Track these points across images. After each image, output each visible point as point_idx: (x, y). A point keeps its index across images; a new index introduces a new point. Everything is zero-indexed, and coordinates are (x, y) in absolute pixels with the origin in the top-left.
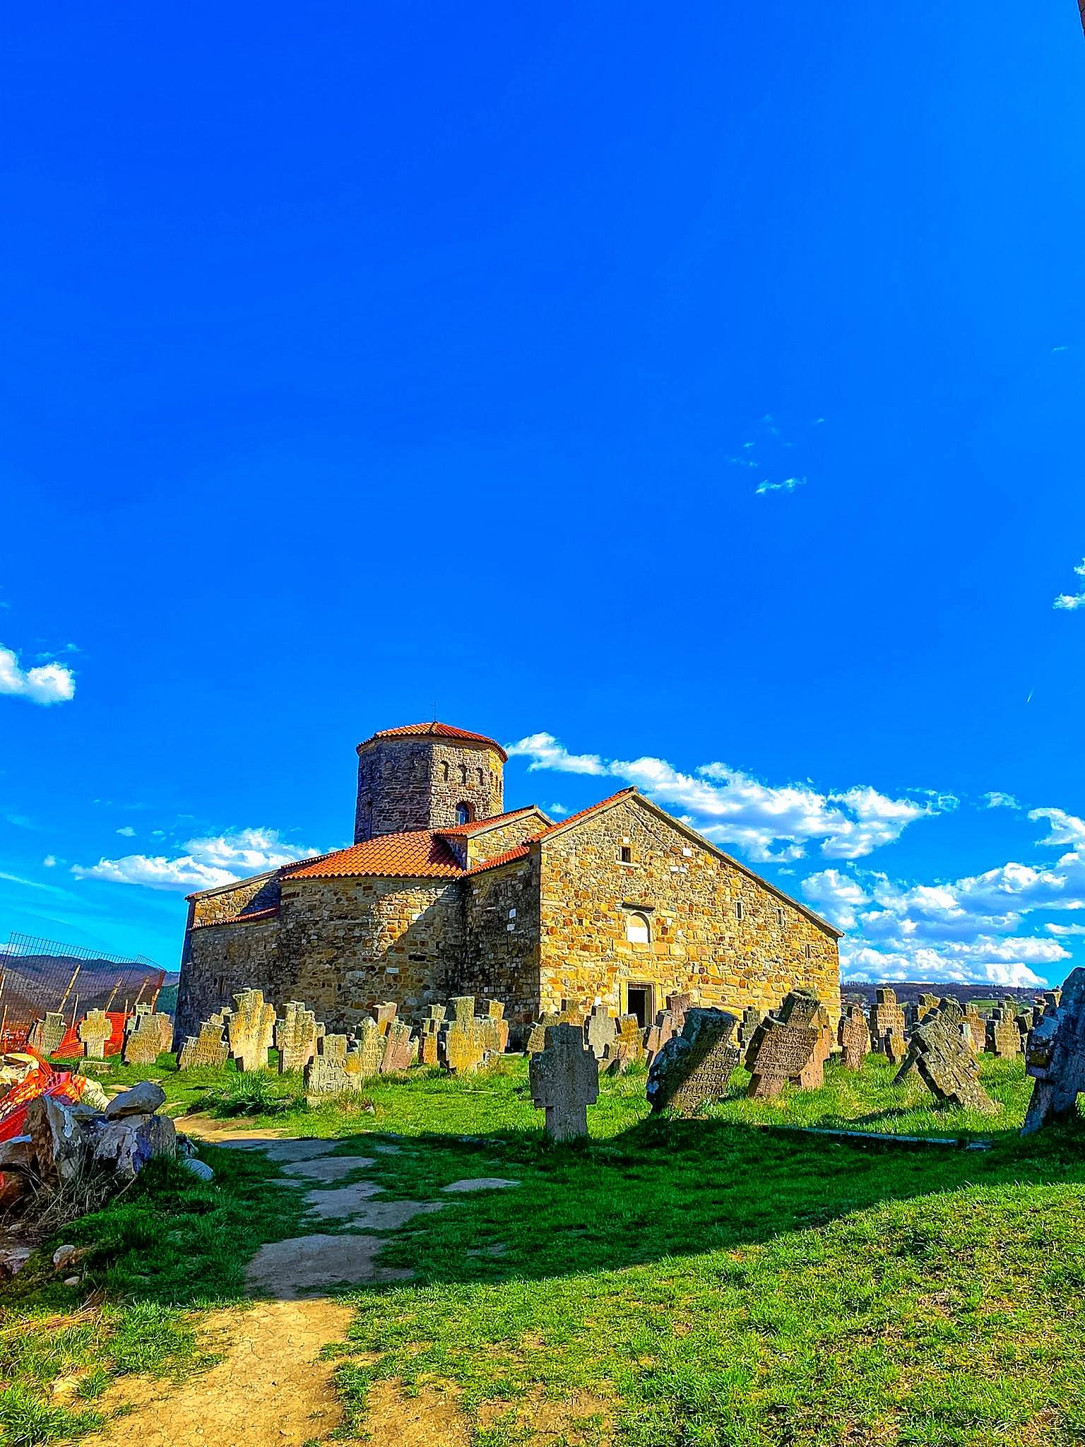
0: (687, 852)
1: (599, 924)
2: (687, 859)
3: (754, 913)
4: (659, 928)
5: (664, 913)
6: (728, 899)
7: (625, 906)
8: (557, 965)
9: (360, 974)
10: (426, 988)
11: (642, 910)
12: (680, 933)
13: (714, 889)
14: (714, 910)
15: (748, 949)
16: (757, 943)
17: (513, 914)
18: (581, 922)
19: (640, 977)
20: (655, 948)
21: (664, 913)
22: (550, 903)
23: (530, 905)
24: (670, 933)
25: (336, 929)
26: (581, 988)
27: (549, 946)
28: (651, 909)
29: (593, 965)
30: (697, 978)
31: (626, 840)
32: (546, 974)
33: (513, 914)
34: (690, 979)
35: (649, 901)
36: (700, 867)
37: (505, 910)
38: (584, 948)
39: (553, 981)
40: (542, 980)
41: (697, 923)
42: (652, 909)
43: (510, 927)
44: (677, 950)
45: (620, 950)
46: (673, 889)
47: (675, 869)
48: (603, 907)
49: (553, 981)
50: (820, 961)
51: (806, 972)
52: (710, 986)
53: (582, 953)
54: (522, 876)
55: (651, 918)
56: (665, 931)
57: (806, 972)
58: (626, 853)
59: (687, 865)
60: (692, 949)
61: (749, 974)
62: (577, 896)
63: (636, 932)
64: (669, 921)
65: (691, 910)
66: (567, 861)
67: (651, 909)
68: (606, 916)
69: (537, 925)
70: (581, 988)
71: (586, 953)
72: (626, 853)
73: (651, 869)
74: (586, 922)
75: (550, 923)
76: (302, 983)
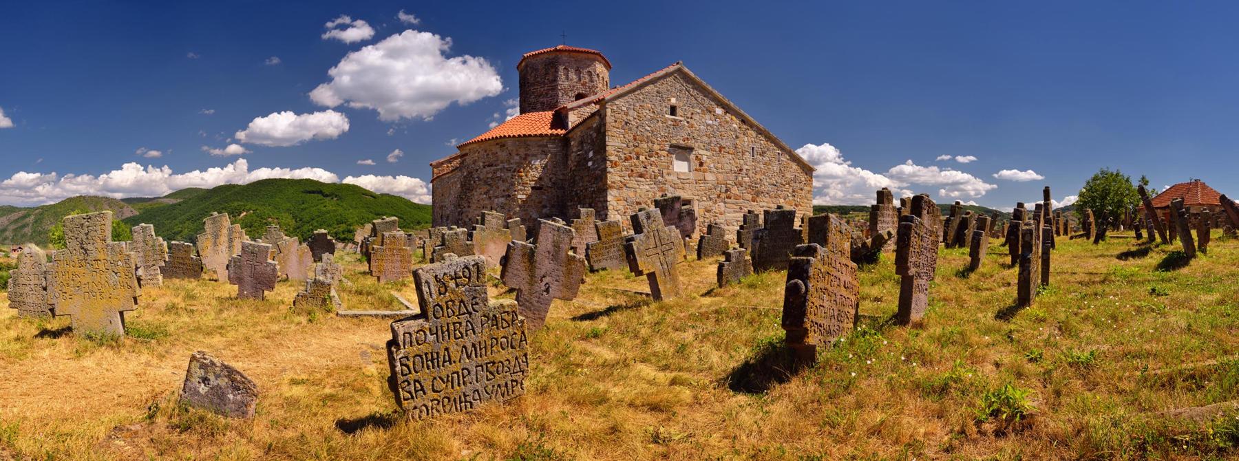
3: (763, 154)
4: (697, 163)
5: (701, 152)
8: (619, 188)
9: (502, 200)
10: (544, 207)
11: (683, 151)
14: (737, 152)
17: (591, 154)
18: (638, 158)
20: (692, 176)
21: (701, 152)
22: (614, 143)
23: (601, 147)
24: (705, 167)
25: (485, 173)
27: (613, 176)
28: (691, 149)
30: (723, 196)
31: (673, 101)
33: (591, 154)
34: (719, 196)
35: (691, 143)
37: (587, 153)
38: (641, 176)
40: (609, 198)
42: (691, 149)
43: (590, 164)
44: (710, 177)
50: (802, 185)
52: (732, 200)
54: (596, 131)
55: (692, 157)
56: (701, 164)
58: (673, 110)
60: (721, 177)
61: (758, 194)
63: (680, 167)
64: (704, 158)
66: (627, 114)
69: (605, 160)
72: (673, 110)
73: (691, 121)
74: (642, 158)
75: (612, 158)
76: (474, 206)
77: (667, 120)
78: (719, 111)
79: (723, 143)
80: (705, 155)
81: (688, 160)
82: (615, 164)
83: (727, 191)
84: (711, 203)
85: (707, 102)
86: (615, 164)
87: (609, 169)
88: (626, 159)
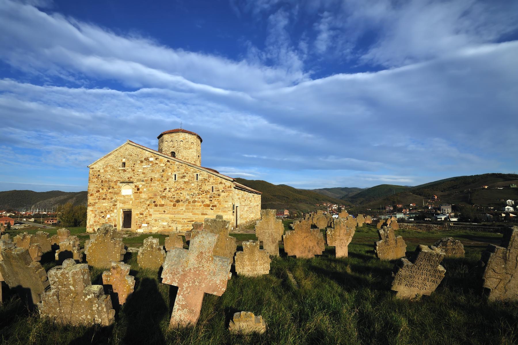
0: (151, 159)
1: (110, 191)
2: (151, 162)
4: (136, 189)
6: (170, 174)
7: (121, 183)
8: (93, 205)
12: (145, 190)
13: (163, 171)
15: (177, 192)
19: (127, 207)
24: (140, 190)
26: (101, 212)
29: (107, 204)
31: (124, 160)
32: (89, 209)
38: (104, 199)
39: (92, 211)
41: (152, 185)
45: (118, 198)
46: (144, 173)
47: (146, 166)
48: (112, 184)
49: (92, 211)
51: (211, 197)
53: (103, 201)
56: (138, 189)
57: (211, 197)
58: (124, 164)
59: (151, 164)
61: (178, 201)
62: (102, 182)
63: (127, 191)
64: (140, 186)
65: (151, 180)
66: (99, 171)
67: (132, 182)
68: (113, 187)
70: (101, 212)
71: (105, 201)
77: (118, 171)
79: (153, 175)
80: (140, 185)
83: (154, 202)
86: (92, 195)
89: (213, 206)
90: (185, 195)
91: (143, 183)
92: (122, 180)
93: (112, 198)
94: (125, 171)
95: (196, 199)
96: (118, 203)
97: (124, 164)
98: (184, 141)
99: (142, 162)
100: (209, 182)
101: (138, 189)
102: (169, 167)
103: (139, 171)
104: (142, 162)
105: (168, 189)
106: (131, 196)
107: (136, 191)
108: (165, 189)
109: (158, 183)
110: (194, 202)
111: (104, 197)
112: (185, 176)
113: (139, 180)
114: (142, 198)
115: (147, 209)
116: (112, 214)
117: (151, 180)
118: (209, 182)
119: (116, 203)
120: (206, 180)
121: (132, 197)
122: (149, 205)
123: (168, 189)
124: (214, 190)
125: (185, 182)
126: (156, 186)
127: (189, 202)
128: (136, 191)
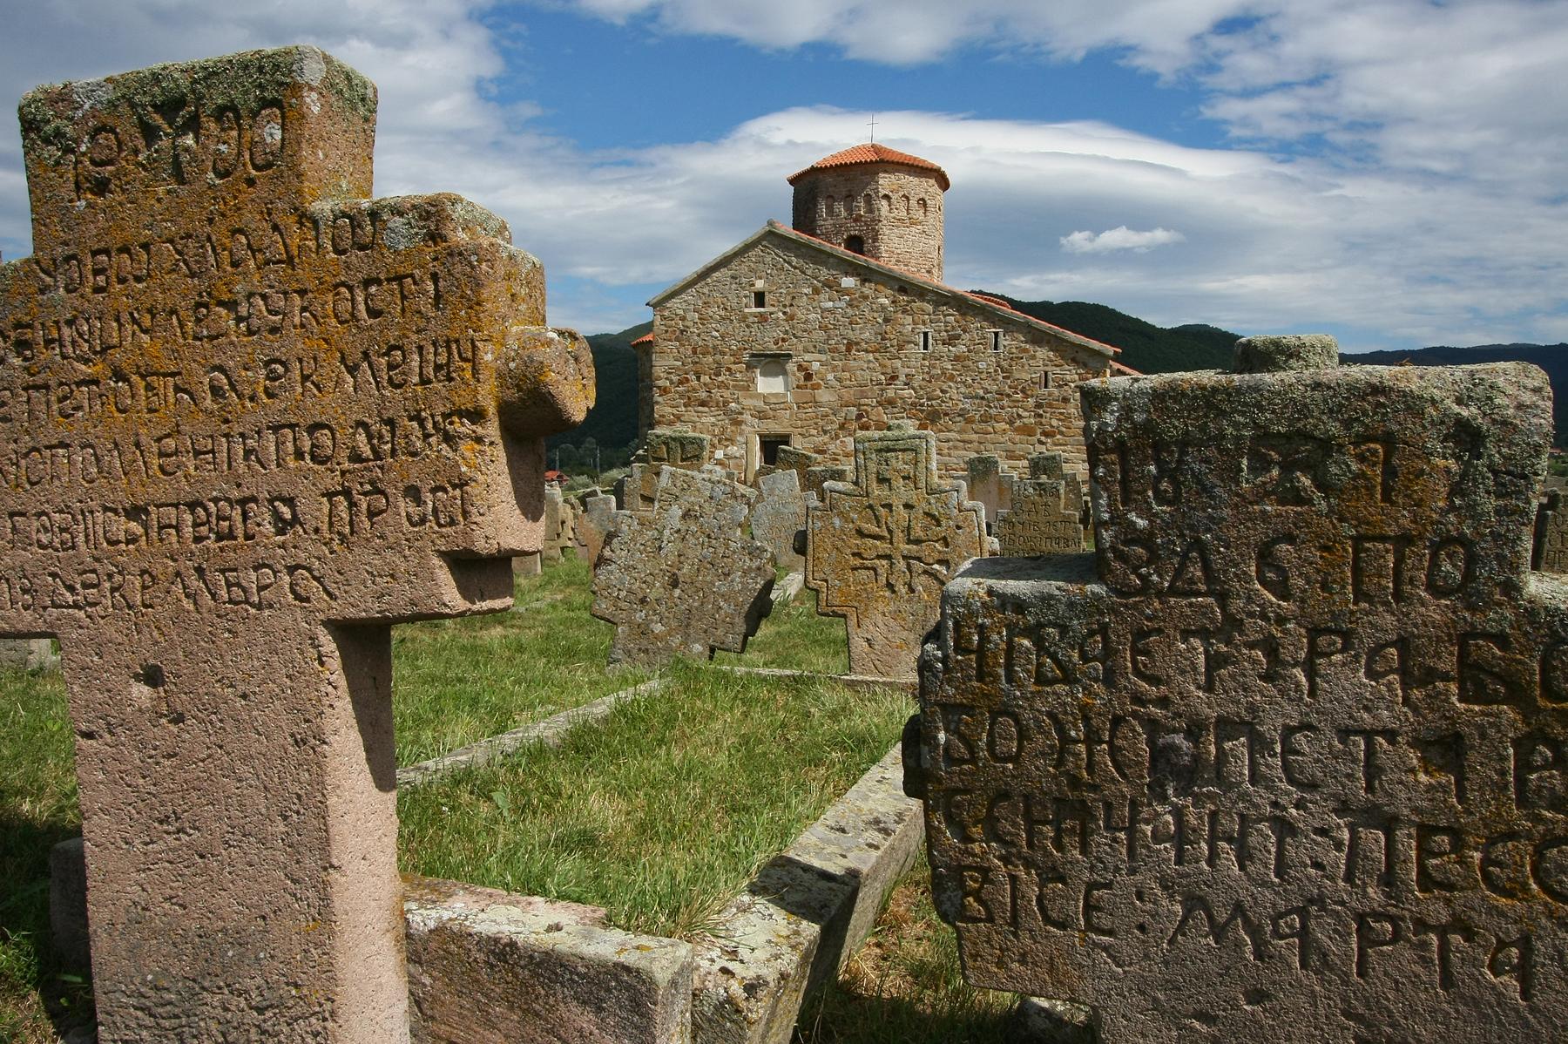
2: (846, 292)
3: (951, 340)
4: (801, 375)
13: (886, 320)
16: (951, 378)
19: (774, 428)
21: (807, 357)
24: (816, 380)
28: (790, 356)
31: (760, 284)
36: (866, 298)
38: (703, 404)
42: (790, 356)
44: (824, 396)
45: (748, 402)
51: (1039, 406)
55: (791, 366)
56: (808, 377)
62: (694, 352)
64: (816, 366)
65: (849, 350)
66: (683, 319)
72: (760, 299)
74: (705, 379)
75: (660, 383)
77: (744, 318)
78: (848, 282)
81: (784, 373)
82: (665, 391)
83: (859, 417)
84: (826, 438)
85: (824, 273)
87: (657, 398)
88: (681, 383)
89: (1045, 434)
90: (955, 397)
91: (823, 357)
92: (757, 349)
93: (726, 403)
94: (763, 319)
95: (993, 411)
96: (747, 417)
97: (760, 299)
98: (894, 197)
99: (816, 291)
100: (1033, 357)
101: (808, 377)
102: (904, 312)
103: (812, 316)
104: (816, 291)
105: (902, 378)
106: (785, 395)
107: (802, 382)
108: (894, 378)
109: (871, 356)
110: (986, 419)
111: (704, 395)
112: (958, 337)
113: (806, 351)
114: (817, 404)
115: (837, 436)
116: (734, 450)
117: (849, 350)
118: (1033, 357)
119: (740, 418)
120: (1025, 350)
121: (789, 398)
122: (842, 427)
123: (902, 378)
124: (1051, 383)
125: (957, 358)
126: (865, 366)
127: (969, 421)
128: (802, 382)
